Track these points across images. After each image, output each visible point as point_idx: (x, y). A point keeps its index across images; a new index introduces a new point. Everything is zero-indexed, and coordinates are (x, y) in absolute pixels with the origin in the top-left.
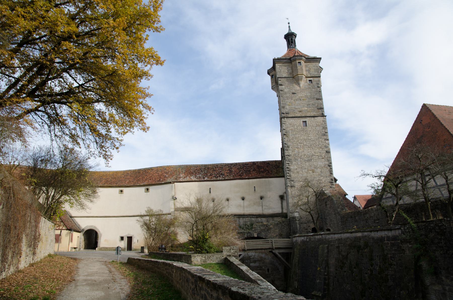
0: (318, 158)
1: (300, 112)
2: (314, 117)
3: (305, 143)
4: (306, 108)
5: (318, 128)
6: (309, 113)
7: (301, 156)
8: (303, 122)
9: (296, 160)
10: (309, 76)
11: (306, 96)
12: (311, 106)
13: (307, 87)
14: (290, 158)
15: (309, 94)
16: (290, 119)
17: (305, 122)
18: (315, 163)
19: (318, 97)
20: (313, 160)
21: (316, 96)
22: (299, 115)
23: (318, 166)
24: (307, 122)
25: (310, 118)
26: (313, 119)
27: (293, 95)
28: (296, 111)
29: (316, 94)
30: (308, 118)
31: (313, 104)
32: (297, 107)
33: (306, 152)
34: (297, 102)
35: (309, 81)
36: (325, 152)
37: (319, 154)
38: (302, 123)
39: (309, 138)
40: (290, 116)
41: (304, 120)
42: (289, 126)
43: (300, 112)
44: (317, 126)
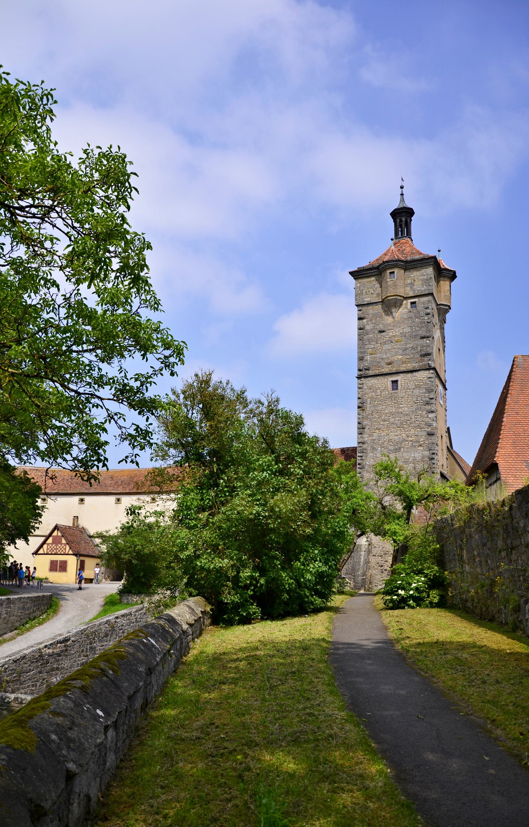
0: (412, 446)
1: (390, 364)
2: (412, 372)
3: (392, 420)
4: (400, 357)
5: (417, 392)
6: (404, 365)
7: (383, 443)
8: (393, 382)
9: (374, 449)
10: (411, 294)
11: (403, 335)
12: (408, 351)
13: (405, 316)
14: (365, 446)
15: (407, 330)
16: (370, 379)
17: (396, 381)
18: (405, 454)
19: (424, 334)
20: (402, 450)
21: (420, 332)
22: (386, 370)
23: (410, 460)
24: (399, 383)
25: (405, 374)
26: (409, 375)
27: (379, 335)
28: (383, 364)
29: (421, 327)
30: (402, 375)
31: (413, 348)
32: (385, 356)
33: (392, 436)
34: (386, 347)
35: (412, 303)
36: (425, 434)
37: (413, 438)
38: (390, 384)
39: (400, 410)
40: (371, 373)
41: (394, 378)
42: (367, 391)
43: (390, 364)
44: (418, 387)
